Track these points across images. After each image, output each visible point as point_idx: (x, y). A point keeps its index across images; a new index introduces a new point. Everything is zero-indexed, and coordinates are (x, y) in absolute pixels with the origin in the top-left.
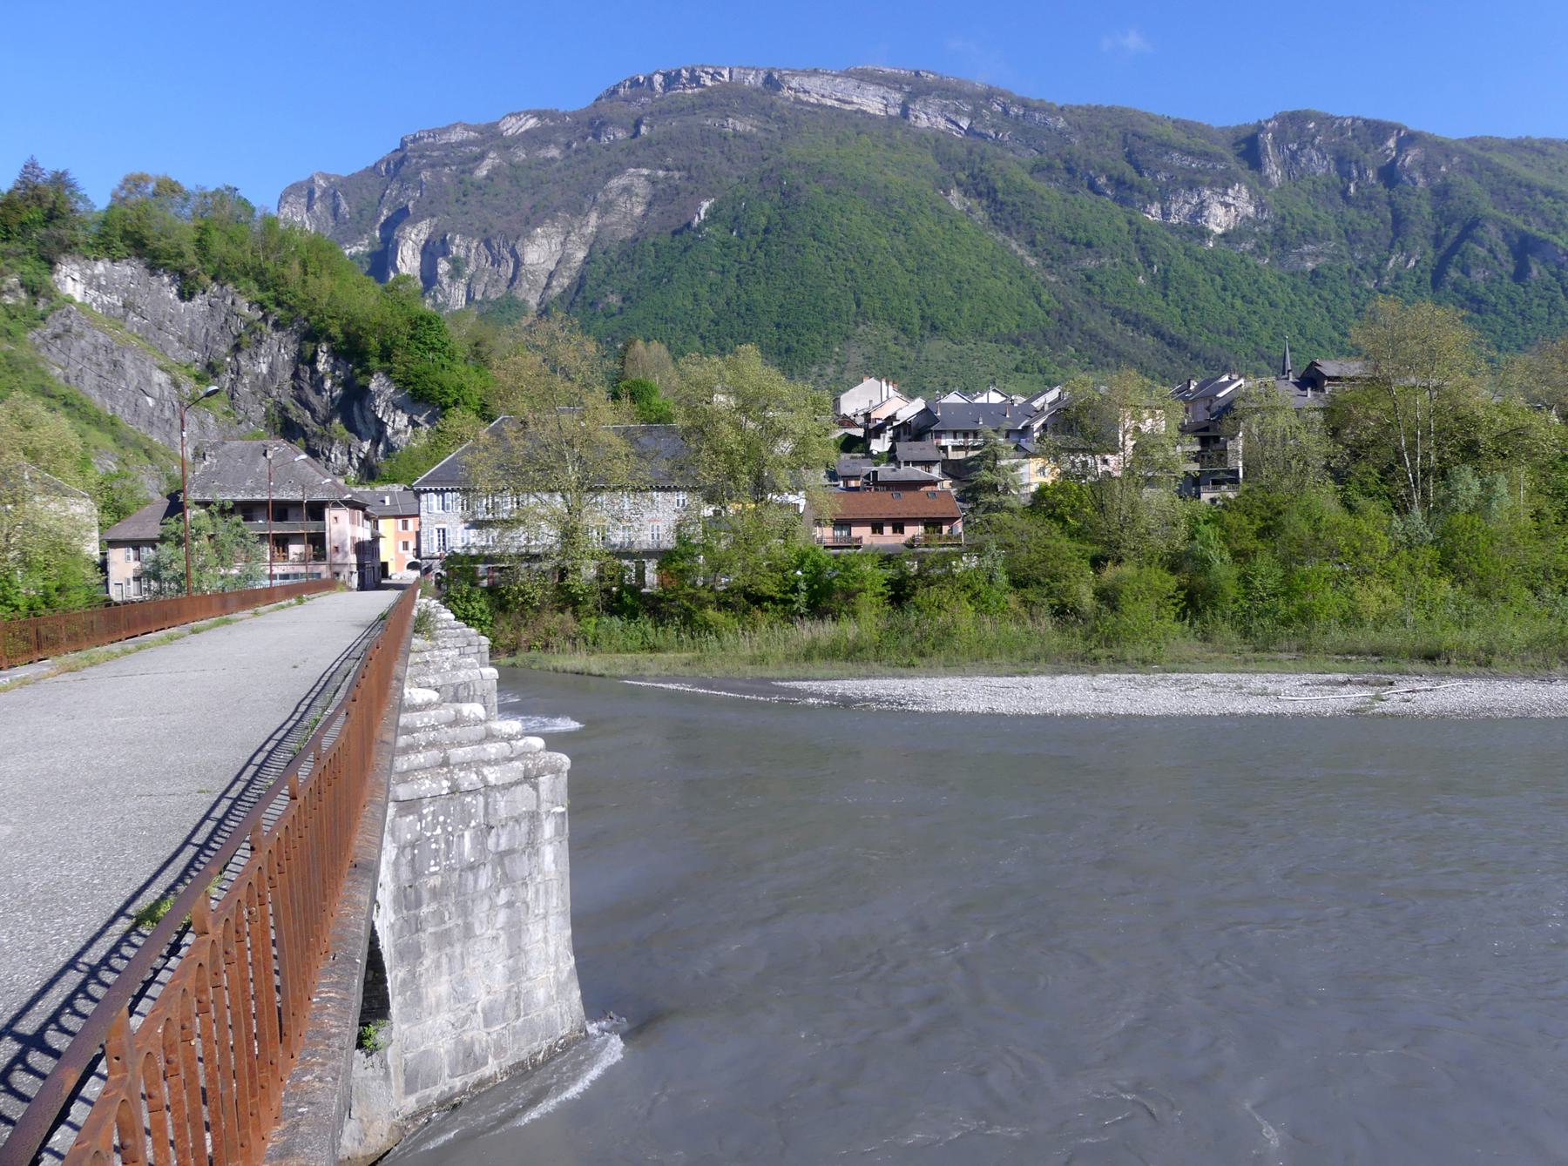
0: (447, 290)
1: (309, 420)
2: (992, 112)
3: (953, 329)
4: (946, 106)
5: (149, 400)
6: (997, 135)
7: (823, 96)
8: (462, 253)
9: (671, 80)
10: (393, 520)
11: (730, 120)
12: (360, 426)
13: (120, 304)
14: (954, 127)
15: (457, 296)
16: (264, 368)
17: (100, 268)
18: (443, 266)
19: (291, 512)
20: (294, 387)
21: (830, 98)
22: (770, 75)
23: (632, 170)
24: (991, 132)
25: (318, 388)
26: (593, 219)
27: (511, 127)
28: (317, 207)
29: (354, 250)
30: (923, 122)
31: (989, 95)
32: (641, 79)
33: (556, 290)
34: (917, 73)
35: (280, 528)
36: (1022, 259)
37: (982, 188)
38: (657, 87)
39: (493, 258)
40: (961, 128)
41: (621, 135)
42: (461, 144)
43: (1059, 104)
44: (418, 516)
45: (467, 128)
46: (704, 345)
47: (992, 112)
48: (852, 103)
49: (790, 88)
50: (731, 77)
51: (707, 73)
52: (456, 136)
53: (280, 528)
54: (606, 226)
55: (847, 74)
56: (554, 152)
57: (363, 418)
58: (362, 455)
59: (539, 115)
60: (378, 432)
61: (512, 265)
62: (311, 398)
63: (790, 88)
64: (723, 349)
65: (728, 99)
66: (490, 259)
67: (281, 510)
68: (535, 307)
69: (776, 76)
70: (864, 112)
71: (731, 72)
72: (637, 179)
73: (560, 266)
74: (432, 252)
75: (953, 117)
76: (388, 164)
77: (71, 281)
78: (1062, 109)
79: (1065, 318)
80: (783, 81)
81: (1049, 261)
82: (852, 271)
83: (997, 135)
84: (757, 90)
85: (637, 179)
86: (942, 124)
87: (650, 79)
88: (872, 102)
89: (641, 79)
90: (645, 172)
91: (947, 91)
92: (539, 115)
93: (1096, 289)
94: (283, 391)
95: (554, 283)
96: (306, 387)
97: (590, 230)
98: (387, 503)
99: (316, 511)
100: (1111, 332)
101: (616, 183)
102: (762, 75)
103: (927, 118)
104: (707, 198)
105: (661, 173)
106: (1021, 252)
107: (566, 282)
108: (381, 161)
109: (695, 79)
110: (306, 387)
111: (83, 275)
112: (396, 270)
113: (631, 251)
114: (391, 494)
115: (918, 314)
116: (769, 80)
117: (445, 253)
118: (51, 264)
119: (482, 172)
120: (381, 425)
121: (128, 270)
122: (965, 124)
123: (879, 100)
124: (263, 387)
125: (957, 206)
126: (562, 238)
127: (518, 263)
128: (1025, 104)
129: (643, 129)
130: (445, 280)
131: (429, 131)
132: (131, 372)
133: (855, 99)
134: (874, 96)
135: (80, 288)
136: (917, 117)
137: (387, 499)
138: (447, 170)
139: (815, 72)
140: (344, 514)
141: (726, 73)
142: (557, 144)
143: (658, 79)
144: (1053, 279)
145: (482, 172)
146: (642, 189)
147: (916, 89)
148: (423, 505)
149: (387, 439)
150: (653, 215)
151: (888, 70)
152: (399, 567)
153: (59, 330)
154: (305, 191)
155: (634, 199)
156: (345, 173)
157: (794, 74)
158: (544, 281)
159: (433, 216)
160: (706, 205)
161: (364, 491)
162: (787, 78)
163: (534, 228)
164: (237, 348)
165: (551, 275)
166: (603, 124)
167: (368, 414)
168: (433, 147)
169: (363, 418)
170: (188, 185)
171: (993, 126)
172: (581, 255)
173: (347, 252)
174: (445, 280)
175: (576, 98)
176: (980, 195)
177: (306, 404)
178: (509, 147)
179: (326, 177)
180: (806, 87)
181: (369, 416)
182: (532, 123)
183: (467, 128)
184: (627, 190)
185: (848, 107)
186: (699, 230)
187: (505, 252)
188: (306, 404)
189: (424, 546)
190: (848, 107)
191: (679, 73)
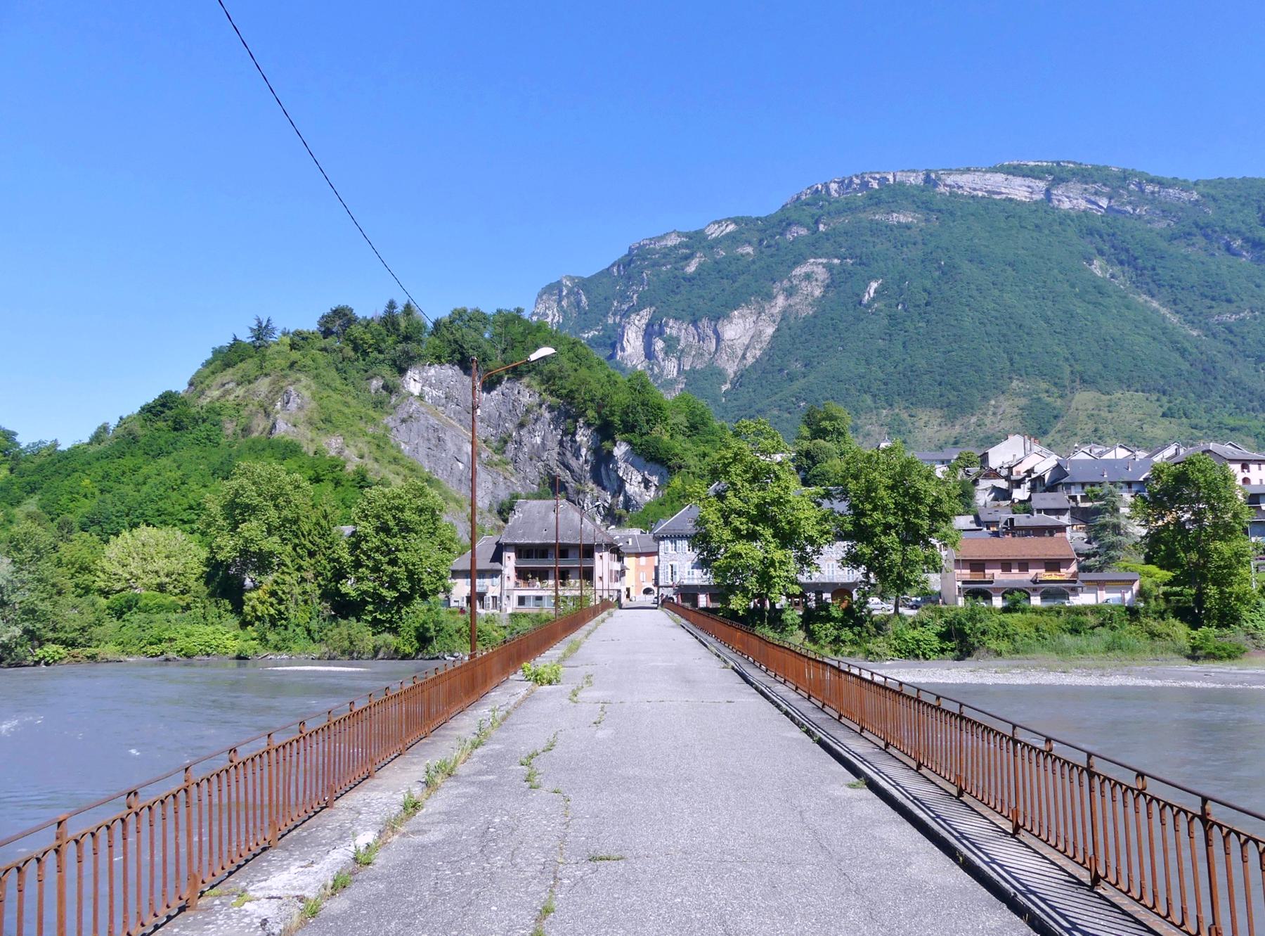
0: (662, 363)
1: (570, 480)
2: (1129, 192)
3: (1100, 380)
4: (1085, 190)
5: (460, 464)
6: (1134, 210)
7: (975, 189)
8: (674, 332)
9: (845, 184)
10: (634, 558)
11: (895, 215)
12: (606, 483)
13: (443, 396)
14: (1095, 207)
15: (671, 368)
16: (538, 440)
17: (432, 371)
18: (659, 345)
19: (570, 553)
20: (559, 454)
21: (981, 190)
22: (928, 176)
23: (812, 260)
24: (1129, 208)
25: (577, 455)
26: (781, 301)
27: (714, 232)
28: (564, 303)
29: (591, 335)
30: (1066, 205)
31: (1125, 176)
32: (820, 187)
33: (750, 360)
34: (1058, 164)
35: (563, 564)
36: (1164, 318)
37: (1123, 256)
38: (833, 193)
39: (699, 335)
40: (1101, 207)
41: (803, 232)
42: (675, 247)
43: (1192, 179)
44: (656, 553)
45: (679, 234)
46: (875, 402)
47: (1129, 192)
48: (1001, 193)
49: (945, 185)
50: (895, 180)
51: (874, 179)
52: (672, 241)
53: (563, 564)
54: (790, 306)
55: (995, 170)
56: (749, 250)
57: (608, 475)
58: (606, 505)
59: (735, 221)
60: (619, 486)
61: (714, 341)
62: (571, 462)
63: (945, 185)
64: (891, 405)
65: (894, 195)
66: (696, 337)
67: (564, 551)
68: (732, 376)
69: (933, 176)
70: (1011, 200)
71: (894, 176)
72: (816, 267)
73: (753, 340)
74: (649, 334)
75: (1093, 198)
76: (619, 266)
77: (413, 383)
78: (1196, 184)
79: (1209, 370)
80: (940, 179)
81: (1191, 317)
82: (1004, 336)
83: (1134, 210)
84: (918, 186)
85: (816, 267)
86: (1083, 204)
87: (826, 186)
88: (1019, 190)
89: (820, 187)
90: (824, 261)
91: (1084, 175)
92: (735, 221)
93: (1237, 340)
94: (552, 455)
95: (748, 354)
96: (569, 455)
97: (776, 310)
98: (630, 543)
99: (588, 551)
100: (1255, 379)
101: (799, 271)
102: (921, 176)
103: (1070, 200)
104: (874, 278)
105: (836, 261)
106: (1163, 310)
107: (758, 353)
108: (613, 265)
109: (865, 185)
110: (567, 453)
111: (421, 378)
112: (623, 349)
113: (809, 325)
114: (633, 537)
115: (1067, 370)
116: (927, 179)
117: (661, 334)
118: (402, 371)
119: (691, 268)
120: (622, 482)
121: (450, 372)
122: (1104, 203)
123: (1025, 189)
124: (536, 455)
125: (1099, 273)
126: (755, 318)
127: (719, 339)
128: (1161, 183)
129: (821, 227)
130: (661, 356)
131: (651, 239)
132: (449, 445)
133: (1003, 190)
134: (1021, 186)
135: (419, 386)
136: (1059, 201)
137: (630, 540)
138: (664, 268)
139: (968, 170)
140: (606, 555)
141: (891, 178)
142: (750, 244)
143: (834, 186)
144: (1195, 333)
145: (691, 268)
146: (821, 274)
147: (1058, 176)
148: (661, 547)
149: (626, 492)
150: (830, 295)
151: (1032, 164)
152: (637, 592)
153: (405, 416)
154: (553, 289)
155: (814, 283)
156: (586, 276)
157: (950, 172)
158: (740, 353)
159: (651, 305)
160: (874, 285)
161: (615, 533)
162: (943, 177)
163: (732, 311)
164: (521, 425)
165: (747, 348)
166: (789, 224)
167: (612, 473)
168: (654, 251)
169: (608, 475)
170: (489, 309)
171: (1130, 203)
172: (770, 331)
173: (586, 336)
174: (661, 356)
175: (767, 205)
176: (1121, 263)
177: (567, 467)
178: (712, 248)
179: (572, 279)
180: (961, 184)
181: (613, 475)
182: (731, 227)
183: (679, 234)
184: (808, 277)
185: (998, 197)
186: (869, 306)
187: (710, 333)
188: (567, 467)
189: (661, 577)
190: (998, 197)
191: (851, 181)
